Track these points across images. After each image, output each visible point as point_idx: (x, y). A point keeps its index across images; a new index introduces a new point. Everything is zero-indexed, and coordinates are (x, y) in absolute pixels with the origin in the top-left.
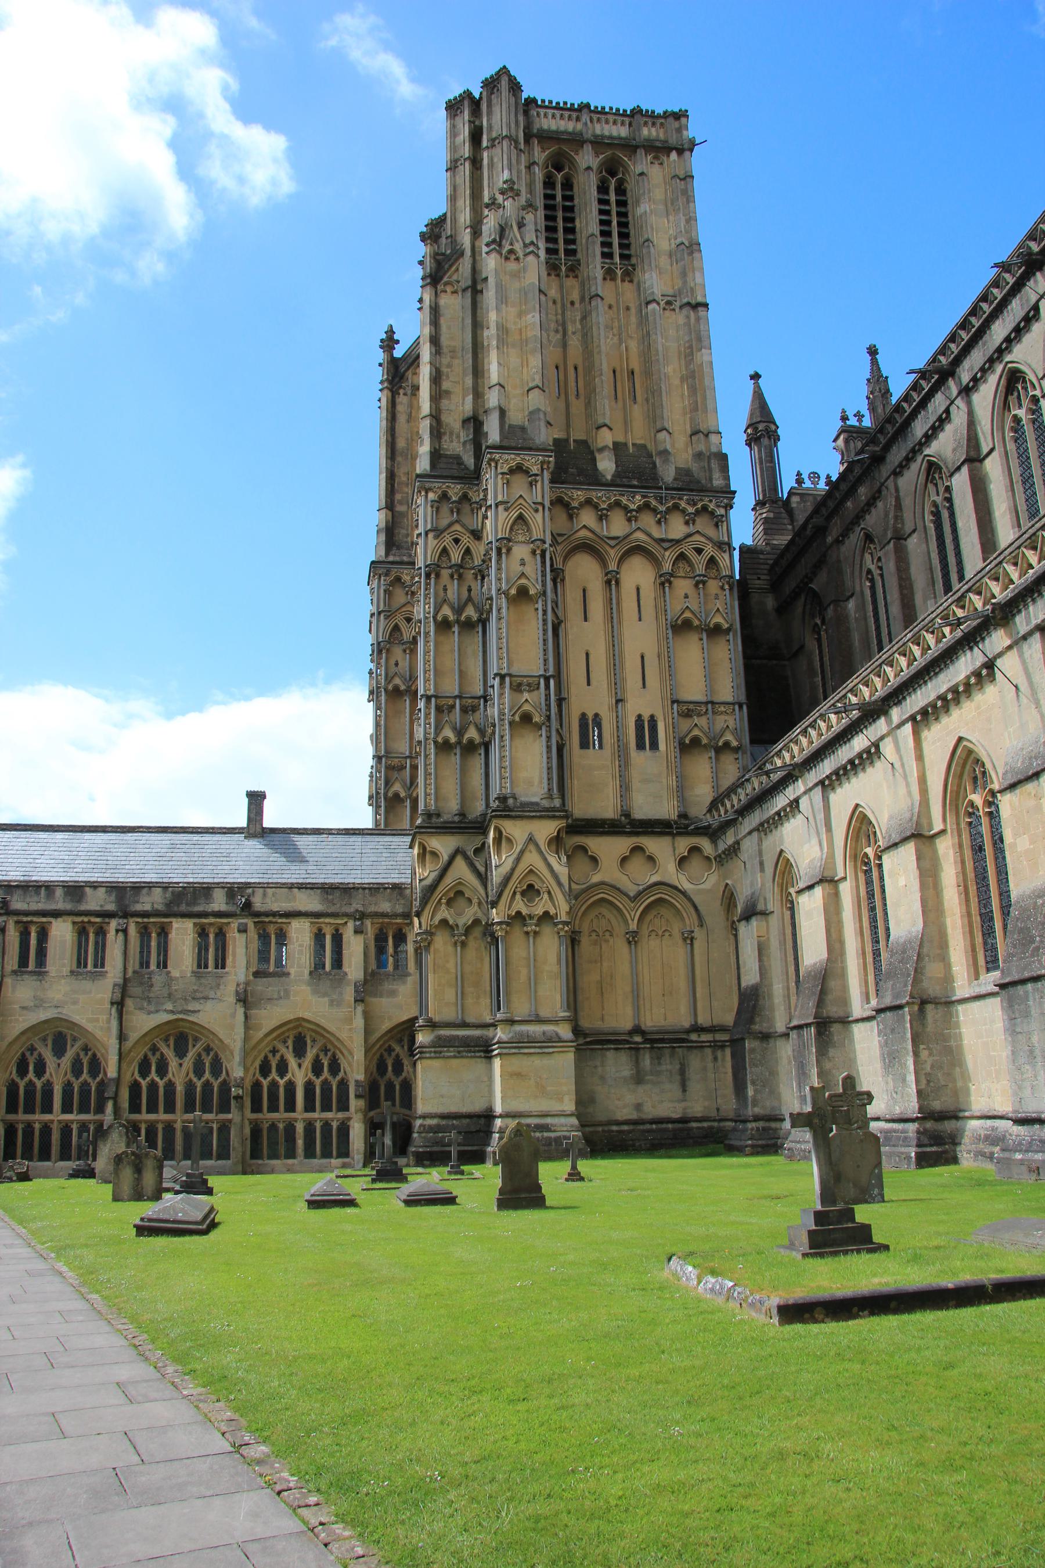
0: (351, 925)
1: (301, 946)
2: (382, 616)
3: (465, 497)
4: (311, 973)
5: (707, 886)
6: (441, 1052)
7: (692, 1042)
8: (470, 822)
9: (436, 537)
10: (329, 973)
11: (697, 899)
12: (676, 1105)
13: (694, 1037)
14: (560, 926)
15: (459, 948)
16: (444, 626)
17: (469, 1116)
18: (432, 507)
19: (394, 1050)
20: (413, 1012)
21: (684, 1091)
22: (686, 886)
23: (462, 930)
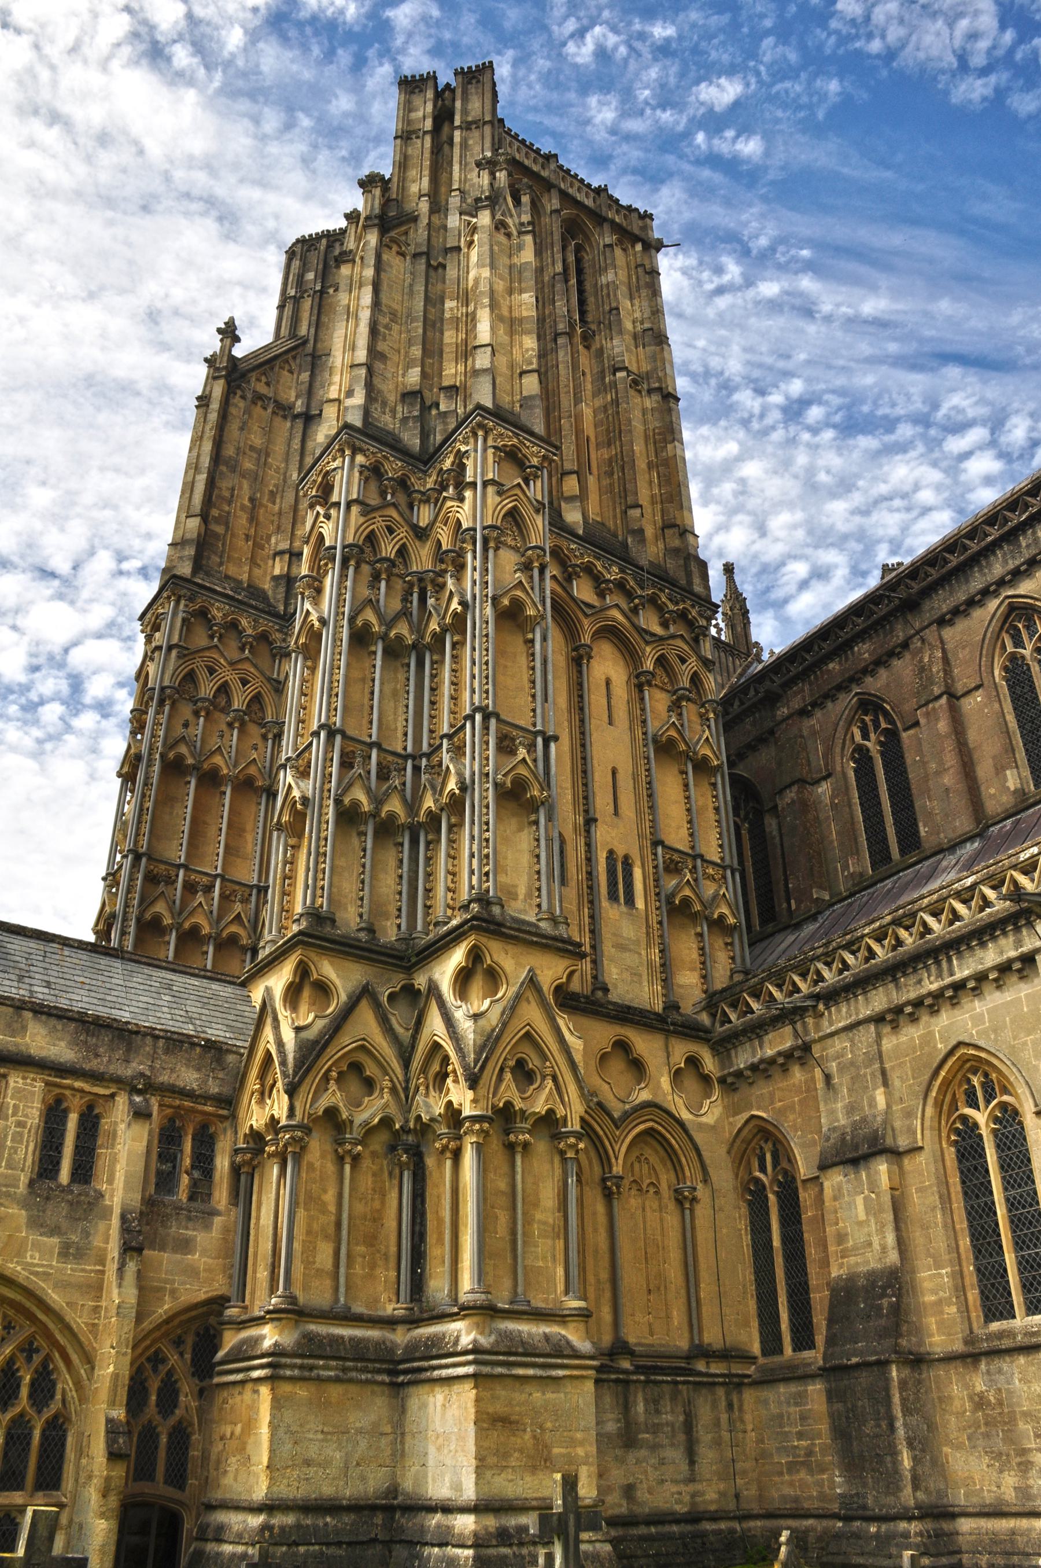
0: (122, 1101)
1: (20, 1124)
2: (174, 653)
3: (403, 483)
4: (31, 1184)
5: (709, 1119)
6: (311, 1368)
7: (700, 1374)
8: (383, 946)
9: (364, 514)
10: (65, 1190)
11: (698, 1138)
12: (682, 1488)
13: (701, 1366)
14: (572, 1140)
15: (347, 1168)
16: (360, 638)
17: (356, 1508)
18: (361, 473)
19: (164, 1360)
20: (219, 1286)
21: (692, 1462)
22: (685, 1115)
23: (356, 1133)
